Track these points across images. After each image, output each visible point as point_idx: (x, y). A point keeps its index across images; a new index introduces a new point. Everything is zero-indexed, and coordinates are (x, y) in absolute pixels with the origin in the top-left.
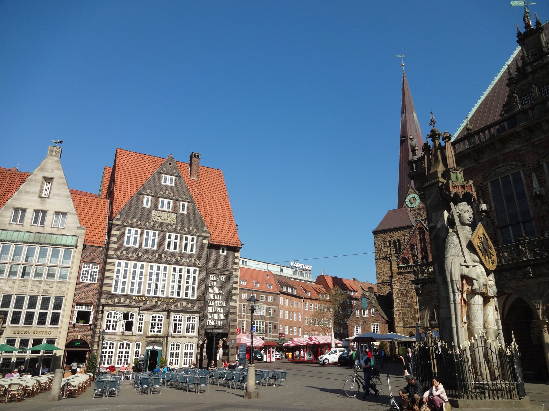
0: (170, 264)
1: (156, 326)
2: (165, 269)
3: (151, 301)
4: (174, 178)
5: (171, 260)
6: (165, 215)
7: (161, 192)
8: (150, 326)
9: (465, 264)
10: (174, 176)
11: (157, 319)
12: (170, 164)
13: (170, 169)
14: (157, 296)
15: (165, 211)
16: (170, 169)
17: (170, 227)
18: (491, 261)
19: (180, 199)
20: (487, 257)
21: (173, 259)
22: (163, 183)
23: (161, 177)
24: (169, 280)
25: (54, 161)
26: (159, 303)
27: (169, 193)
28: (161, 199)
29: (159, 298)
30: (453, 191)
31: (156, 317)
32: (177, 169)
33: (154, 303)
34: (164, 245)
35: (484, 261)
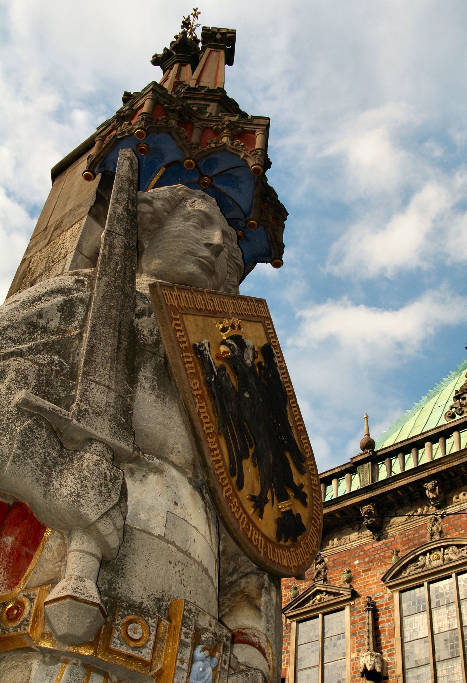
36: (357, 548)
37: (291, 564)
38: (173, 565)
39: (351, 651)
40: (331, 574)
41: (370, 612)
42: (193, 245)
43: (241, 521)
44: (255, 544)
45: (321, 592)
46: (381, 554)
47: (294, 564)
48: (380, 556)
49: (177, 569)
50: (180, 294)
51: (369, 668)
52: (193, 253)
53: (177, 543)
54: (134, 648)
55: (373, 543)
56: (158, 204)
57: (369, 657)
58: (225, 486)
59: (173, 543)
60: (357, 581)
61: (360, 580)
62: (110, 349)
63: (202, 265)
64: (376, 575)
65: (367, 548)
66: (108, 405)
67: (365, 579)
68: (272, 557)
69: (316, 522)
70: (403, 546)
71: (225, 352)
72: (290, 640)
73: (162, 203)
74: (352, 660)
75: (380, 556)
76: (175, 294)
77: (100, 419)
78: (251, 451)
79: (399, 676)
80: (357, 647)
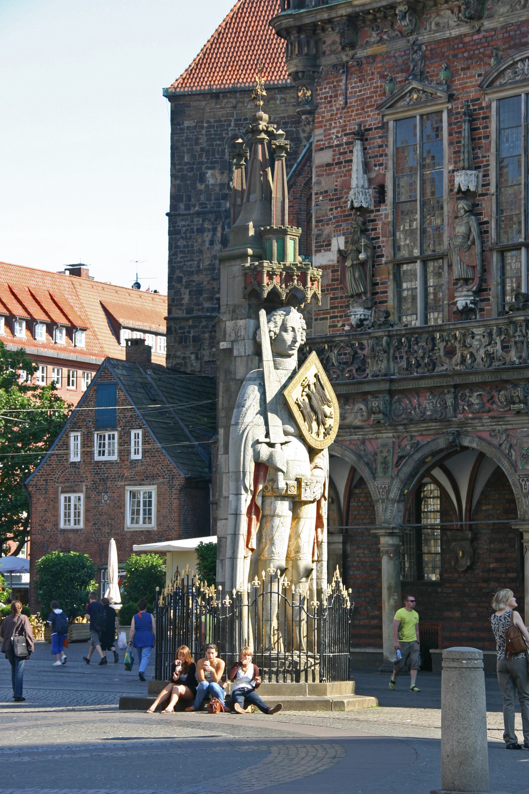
9: (267, 440)
18: (322, 430)
20: (314, 424)
30: (268, 285)
35: (305, 432)
36: (456, 38)
39: (449, 162)
40: (429, 68)
41: (467, 123)
45: (419, 90)
46: (481, 50)
48: (480, 53)
51: (463, 189)
55: (473, 35)
57: (463, 177)
60: (455, 80)
61: (458, 80)
64: (474, 76)
65: (467, 39)
67: (463, 79)
70: (504, 44)
72: (387, 141)
74: (449, 172)
75: (480, 53)
79: (493, 195)
80: (454, 157)
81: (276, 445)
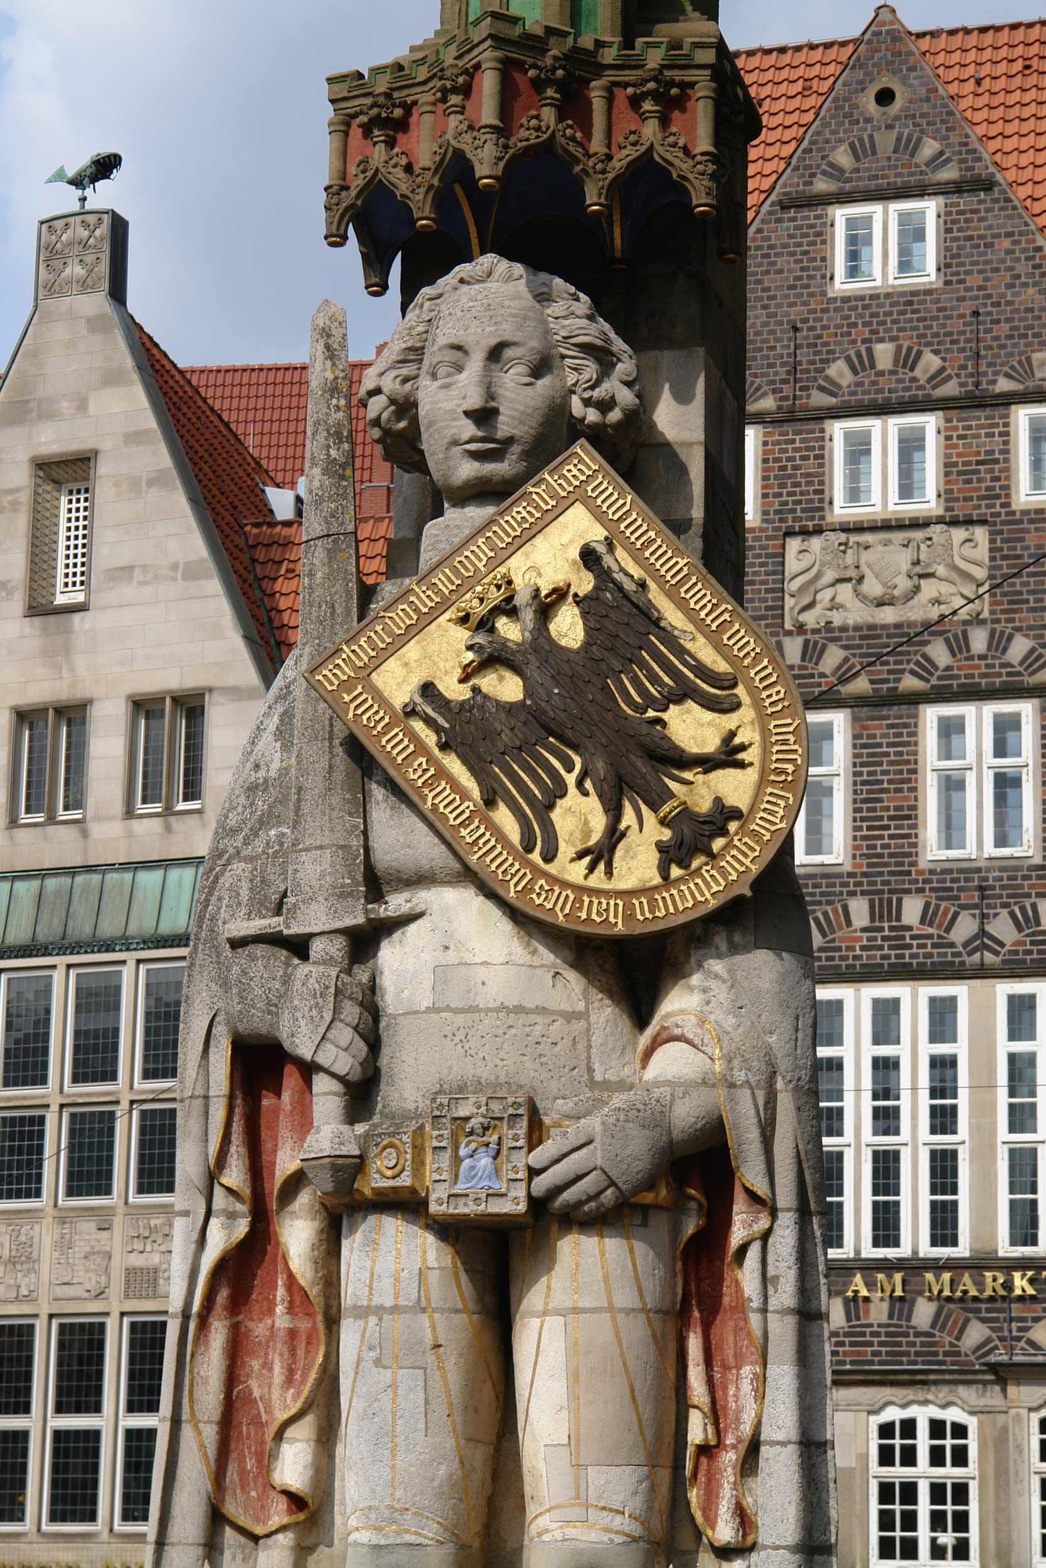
0: (982, 973)
1: (924, 1507)
2: (942, 1017)
3: (854, 1305)
4: (930, 208)
5: (982, 939)
6: (890, 560)
7: (838, 370)
8: (874, 1507)
10: (921, 191)
11: (923, 1443)
12: (885, 97)
13: (885, 142)
14: (904, 1251)
15: (886, 526)
16: (885, 142)
17: (939, 653)
19: (1004, 385)
21: (1002, 928)
22: (841, 284)
23: (822, 235)
24: (983, 1110)
25: (82, 328)
26: (923, 1312)
27: (907, 360)
28: (838, 429)
29: (913, 1267)
31: (909, 1428)
32: (947, 120)
33: (878, 1313)
34: (909, 815)
37: (703, 895)
38: (450, 1036)
42: (448, 427)
43: (558, 909)
44: (598, 920)
47: (715, 889)
49: (457, 1039)
50: (355, 647)
52: (455, 443)
53: (453, 1006)
54: (394, 1178)
56: (389, 384)
58: (513, 875)
59: (448, 1009)
62: (320, 779)
63: (477, 456)
66: (323, 875)
68: (648, 915)
69: (783, 772)
71: (468, 665)
73: (394, 373)
76: (344, 656)
77: (314, 906)
78: (571, 779)
81: (317, 947)
